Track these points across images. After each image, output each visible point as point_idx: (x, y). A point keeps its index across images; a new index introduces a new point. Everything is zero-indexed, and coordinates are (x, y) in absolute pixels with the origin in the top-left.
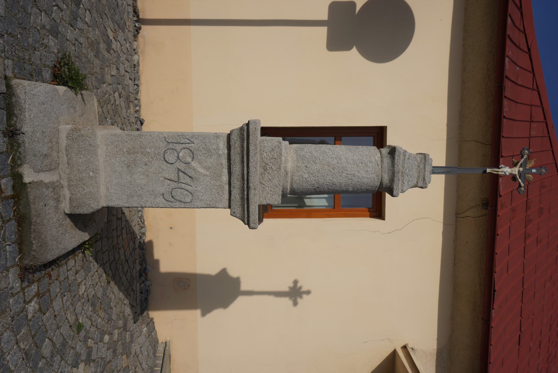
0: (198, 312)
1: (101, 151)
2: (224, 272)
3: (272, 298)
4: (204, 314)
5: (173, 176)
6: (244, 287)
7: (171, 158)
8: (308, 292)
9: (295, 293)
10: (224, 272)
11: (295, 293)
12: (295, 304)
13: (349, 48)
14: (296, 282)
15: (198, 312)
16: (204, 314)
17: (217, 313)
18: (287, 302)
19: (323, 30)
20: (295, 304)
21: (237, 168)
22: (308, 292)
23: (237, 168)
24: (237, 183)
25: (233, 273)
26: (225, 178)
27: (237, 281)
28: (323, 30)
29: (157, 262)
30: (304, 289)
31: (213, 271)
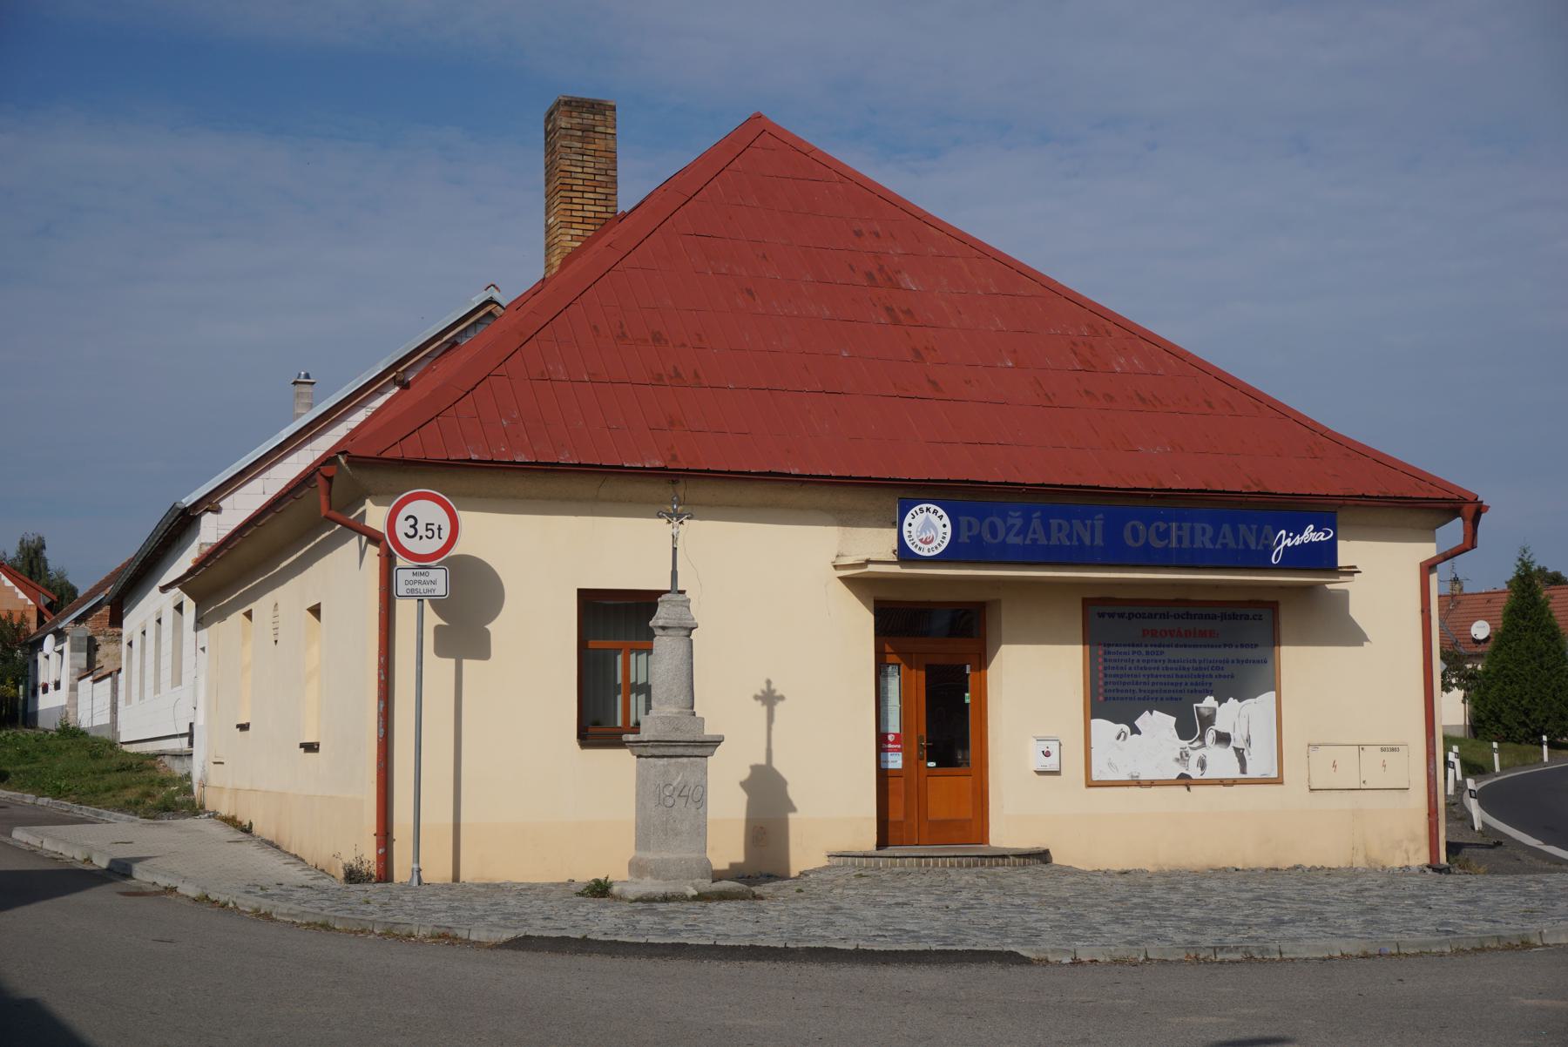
0: (791, 816)
1: (665, 855)
2: (744, 785)
3: (774, 726)
4: (794, 810)
5: (683, 800)
6: (762, 761)
7: (670, 802)
8: (769, 682)
9: (769, 698)
10: (744, 785)
11: (769, 698)
12: (782, 698)
13: (488, 633)
14: (756, 698)
15: (791, 816)
16: (794, 810)
17: (793, 793)
18: (779, 708)
19: (466, 663)
20: (782, 698)
21: (679, 751)
22: (769, 682)
23: (679, 751)
24: (690, 751)
25: (745, 773)
26: (685, 760)
27: (755, 769)
28: (466, 663)
29: (732, 865)
30: (764, 687)
31: (742, 797)
